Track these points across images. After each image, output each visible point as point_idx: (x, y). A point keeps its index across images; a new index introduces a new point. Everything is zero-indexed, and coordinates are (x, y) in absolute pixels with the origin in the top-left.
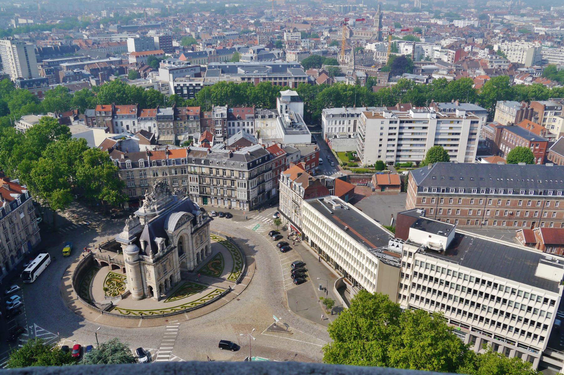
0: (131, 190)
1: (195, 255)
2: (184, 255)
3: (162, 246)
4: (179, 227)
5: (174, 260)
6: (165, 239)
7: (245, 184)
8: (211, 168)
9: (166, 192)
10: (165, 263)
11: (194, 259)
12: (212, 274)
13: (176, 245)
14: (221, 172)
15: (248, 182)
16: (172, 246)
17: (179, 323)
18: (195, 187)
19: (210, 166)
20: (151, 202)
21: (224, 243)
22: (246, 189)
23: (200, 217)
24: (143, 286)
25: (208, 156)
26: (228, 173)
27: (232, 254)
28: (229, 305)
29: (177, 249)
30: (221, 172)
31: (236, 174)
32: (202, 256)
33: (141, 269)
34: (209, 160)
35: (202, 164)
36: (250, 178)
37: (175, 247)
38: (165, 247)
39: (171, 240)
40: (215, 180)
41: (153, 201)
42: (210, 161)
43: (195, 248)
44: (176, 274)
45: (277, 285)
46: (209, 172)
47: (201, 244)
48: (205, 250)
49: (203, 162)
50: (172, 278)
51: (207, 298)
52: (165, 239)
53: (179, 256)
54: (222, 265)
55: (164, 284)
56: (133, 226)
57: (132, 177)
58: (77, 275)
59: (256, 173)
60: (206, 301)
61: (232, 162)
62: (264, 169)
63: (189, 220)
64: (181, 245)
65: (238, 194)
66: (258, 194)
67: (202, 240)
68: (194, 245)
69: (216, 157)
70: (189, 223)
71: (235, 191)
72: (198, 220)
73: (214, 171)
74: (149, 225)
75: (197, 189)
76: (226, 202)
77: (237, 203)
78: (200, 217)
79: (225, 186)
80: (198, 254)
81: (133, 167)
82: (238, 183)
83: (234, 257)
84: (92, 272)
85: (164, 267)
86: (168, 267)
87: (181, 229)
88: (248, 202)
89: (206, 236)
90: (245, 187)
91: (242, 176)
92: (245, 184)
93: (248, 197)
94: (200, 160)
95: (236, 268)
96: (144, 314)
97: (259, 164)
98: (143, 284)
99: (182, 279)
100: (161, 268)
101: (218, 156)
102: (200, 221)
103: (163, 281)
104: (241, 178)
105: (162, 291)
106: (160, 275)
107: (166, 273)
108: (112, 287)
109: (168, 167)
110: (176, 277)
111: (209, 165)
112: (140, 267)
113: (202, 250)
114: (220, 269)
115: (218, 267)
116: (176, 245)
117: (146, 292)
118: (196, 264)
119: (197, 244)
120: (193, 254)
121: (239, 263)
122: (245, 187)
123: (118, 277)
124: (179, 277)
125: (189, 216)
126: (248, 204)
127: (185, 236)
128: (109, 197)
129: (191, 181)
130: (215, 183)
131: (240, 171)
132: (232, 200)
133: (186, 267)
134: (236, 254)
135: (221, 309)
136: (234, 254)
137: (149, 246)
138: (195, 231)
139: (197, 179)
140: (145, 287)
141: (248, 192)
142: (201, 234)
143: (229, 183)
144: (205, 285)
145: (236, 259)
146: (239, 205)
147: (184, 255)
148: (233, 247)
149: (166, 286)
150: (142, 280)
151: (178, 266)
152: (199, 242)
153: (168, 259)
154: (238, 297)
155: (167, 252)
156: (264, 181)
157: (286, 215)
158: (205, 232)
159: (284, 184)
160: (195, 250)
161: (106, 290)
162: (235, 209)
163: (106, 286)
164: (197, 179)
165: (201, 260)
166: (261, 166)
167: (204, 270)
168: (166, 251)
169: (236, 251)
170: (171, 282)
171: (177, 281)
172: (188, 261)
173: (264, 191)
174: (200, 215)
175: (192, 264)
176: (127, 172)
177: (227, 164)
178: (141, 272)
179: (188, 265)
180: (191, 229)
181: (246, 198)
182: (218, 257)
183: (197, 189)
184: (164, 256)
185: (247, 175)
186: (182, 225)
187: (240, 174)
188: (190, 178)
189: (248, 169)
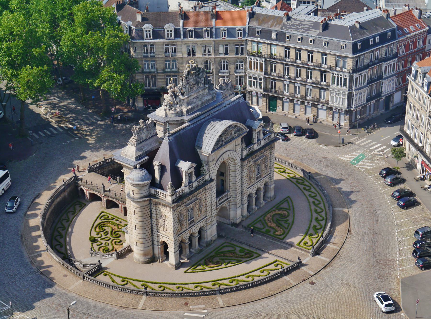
0: (148, 77)
1: (245, 198)
2: (227, 195)
3: (190, 175)
4: (221, 146)
5: (208, 202)
6: (195, 165)
7: (345, 80)
8: (288, 48)
9: (204, 84)
10: (191, 206)
11: (242, 205)
12: (271, 233)
13: (214, 177)
14: (304, 56)
15: (351, 77)
16: (207, 177)
17: (206, 311)
18: (256, 79)
19: (286, 45)
20: (178, 100)
21: (297, 182)
22: (347, 88)
23: (259, 132)
24: (153, 241)
25: (284, 25)
26: (317, 57)
27: (309, 202)
28: (294, 289)
29: (214, 184)
30: (304, 56)
31: (331, 61)
32: (257, 199)
33: (151, 211)
34: (284, 34)
35: (272, 39)
36: (356, 70)
37: (212, 180)
38: (194, 178)
39: (206, 168)
40: (292, 69)
41: (181, 97)
42: (287, 35)
43: (245, 185)
44: (209, 227)
45: (384, 265)
46: (283, 55)
47: (257, 178)
48: (263, 190)
49: (274, 35)
50: (203, 233)
51: (258, 273)
52: (195, 165)
53: (217, 196)
54: (290, 219)
55: (187, 241)
56: (144, 138)
57: (152, 54)
58: (50, 210)
59: (366, 61)
60: (256, 279)
61: (326, 39)
62: (384, 56)
63: (239, 135)
64: (222, 178)
65: (332, 97)
66: (368, 100)
67: (258, 173)
68: (245, 179)
69: (298, 29)
70: (239, 140)
71: (326, 92)
72: (255, 136)
73: (293, 53)
74: (171, 138)
75: (260, 84)
76: (309, 110)
77: (328, 114)
78: (259, 132)
79: (309, 81)
80: (250, 196)
81: (154, 38)
82: (334, 78)
83: (313, 207)
84: (75, 209)
85: (191, 212)
86: (196, 213)
87: (224, 149)
88: (349, 112)
89: (266, 166)
90: (345, 85)
91: (340, 65)
92: (345, 80)
93: (349, 104)
94: (270, 32)
95: (315, 227)
96: (150, 287)
97: (375, 45)
98: (153, 238)
99: (220, 236)
100: (185, 214)
101: (302, 27)
102: (258, 140)
103: (186, 236)
104: (339, 69)
105: (184, 253)
106: (181, 226)
107: (192, 223)
108: (104, 237)
109: (214, 41)
110: (209, 232)
111: (285, 41)
112: (151, 208)
113: (258, 190)
114: (286, 225)
115: (282, 223)
116: (214, 177)
117: (156, 252)
118: (245, 213)
119: (250, 178)
120: (242, 194)
121: (321, 218)
122: (345, 85)
123: (114, 221)
124: (215, 233)
125: (240, 129)
126: (347, 117)
127: (231, 163)
128: (111, 84)
129: (250, 67)
130: (292, 74)
131: (337, 56)
132: (319, 107)
133: (228, 217)
134: (317, 202)
135: (280, 296)
136: (314, 203)
137: (168, 175)
138: (248, 156)
139: (261, 64)
140: (156, 243)
141: (350, 96)
142: (259, 162)
143: (317, 76)
144: (258, 251)
145: (316, 211)
146: (331, 116)
147: (227, 195)
148: (313, 190)
149: (191, 245)
150: (152, 231)
151: (215, 212)
152: (254, 175)
153: (197, 199)
154: (313, 279)
155: (198, 188)
156: (380, 77)
157: (416, 141)
158: (267, 158)
159: (417, 84)
160: (245, 189)
161: (93, 240)
162: (324, 122)
163: (94, 234)
164: (261, 64)
165: (254, 207)
166: (377, 50)
167: (259, 225)
168: (195, 185)
169: (318, 198)
170: (200, 239)
171: (209, 239)
172: (232, 206)
173: (379, 94)
174: (258, 130)
175: (239, 212)
176: (145, 46)
177: (315, 42)
178: (151, 217)
179: (232, 214)
180: (242, 151)
181: (345, 106)
182: (285, 205)
183: (260, 84)
184: (191, 193)
185: (350, 64)
186: (227, 143)
187: (337, 61)
188: (250, 62)
189: (354, 53)
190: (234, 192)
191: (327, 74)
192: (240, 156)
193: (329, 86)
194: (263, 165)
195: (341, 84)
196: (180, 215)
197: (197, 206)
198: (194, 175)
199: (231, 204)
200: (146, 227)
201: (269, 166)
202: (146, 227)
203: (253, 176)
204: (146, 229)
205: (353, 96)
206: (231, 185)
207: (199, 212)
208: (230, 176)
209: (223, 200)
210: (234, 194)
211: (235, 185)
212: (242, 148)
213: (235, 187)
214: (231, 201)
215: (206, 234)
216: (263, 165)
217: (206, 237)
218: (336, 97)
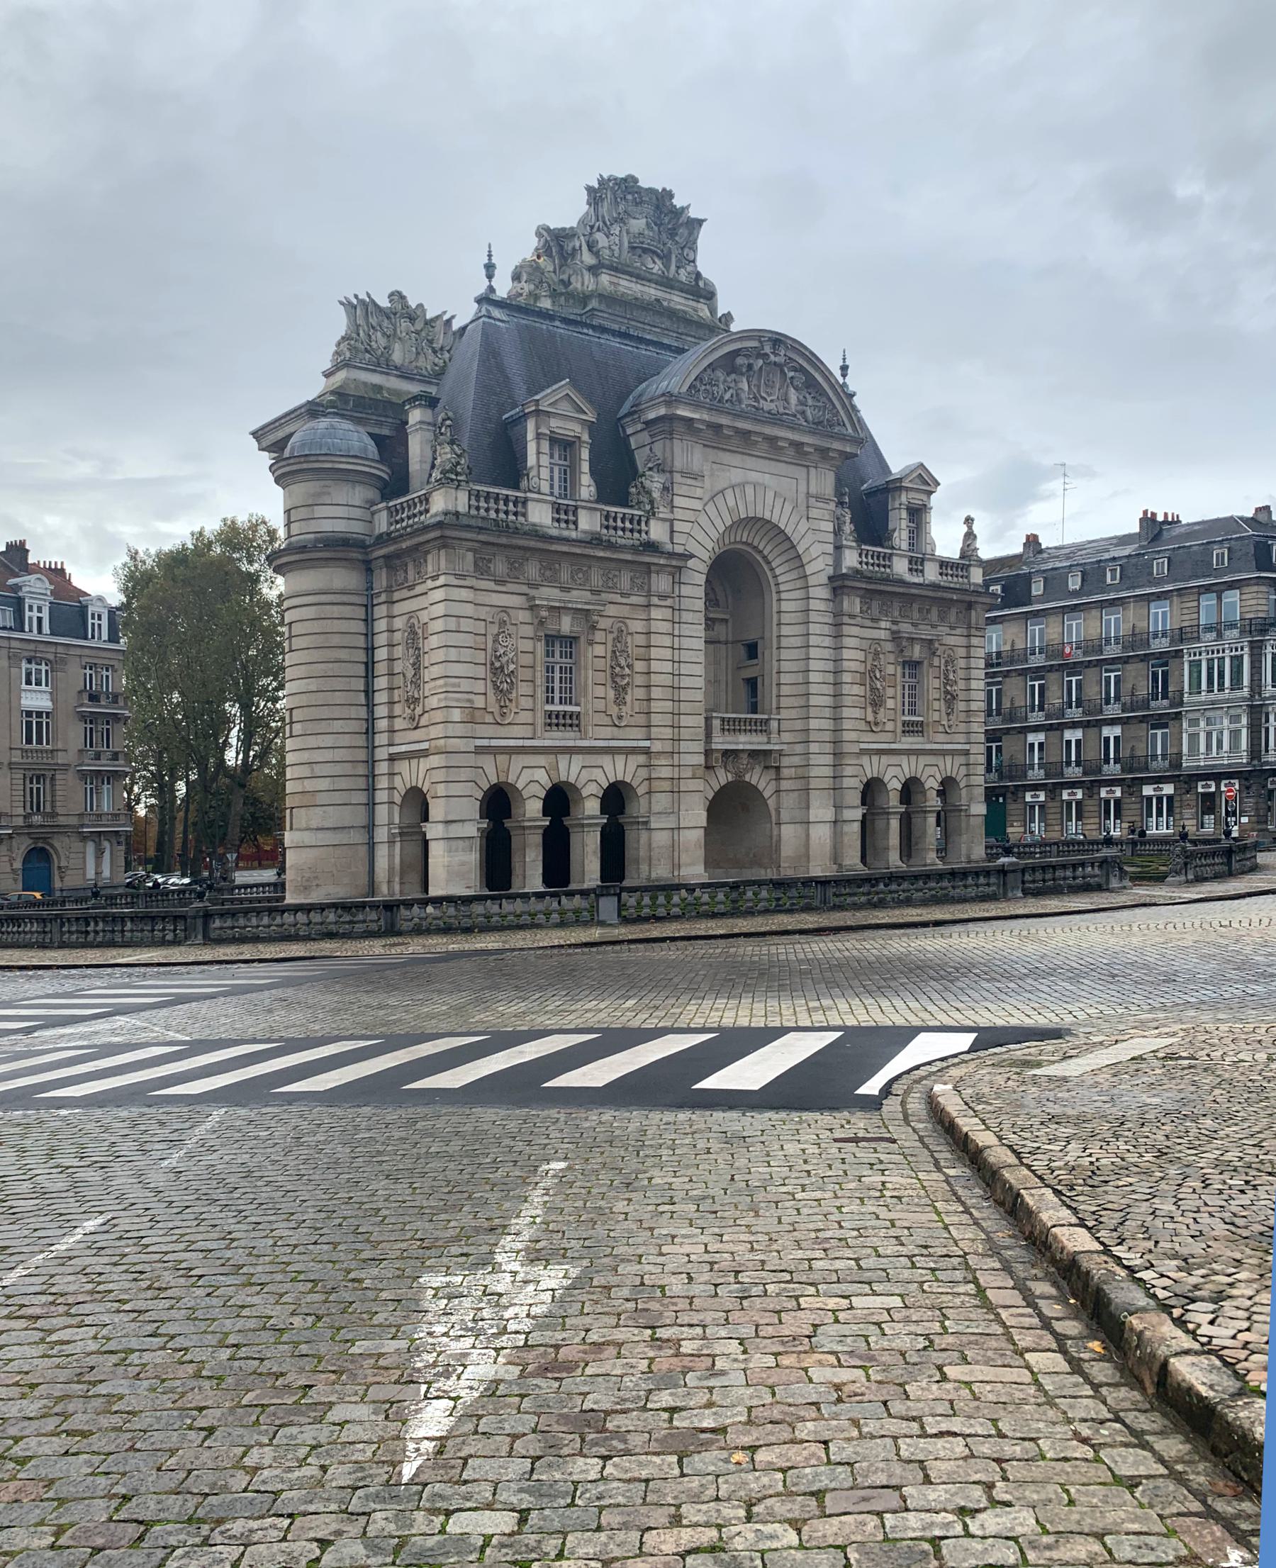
7: (1237, 661)
22: (1246, 692)
39: (655, 483)
44: (661, 801)
65: (1194, 738)
80: (871, 789)
82: (1196, 665)
89: (950, 699)
92: (1237, 661)
119: (876, 702)
127: (784, 575)
171: (661, 872)
179: (789, 834)
190: (799, 725)
191: (1173, 663)
192: (830, 561)
193: (1181, 704)
194: (936, 683)
195: (1221, 684)
196: (494, 629)
197: (599, 650)
198: (585, 467)
199: (785, 785)
200: (337, 712)
201: (962, 706)
202: (337, 712)
203: (890, 703)
204: (338, 726)
205: (1267, 721)
206: (785, 690)
207: (611, 694)
208: (784, 642)
209: (743, 738)
210: (800, 737)
211: (801, 689)
212: (837, 532)
213: (801, 702)
214: (785, 773)
215: (644, 836)
216: (936, 683)
217: (643, 853)
218: (1209, 735)
